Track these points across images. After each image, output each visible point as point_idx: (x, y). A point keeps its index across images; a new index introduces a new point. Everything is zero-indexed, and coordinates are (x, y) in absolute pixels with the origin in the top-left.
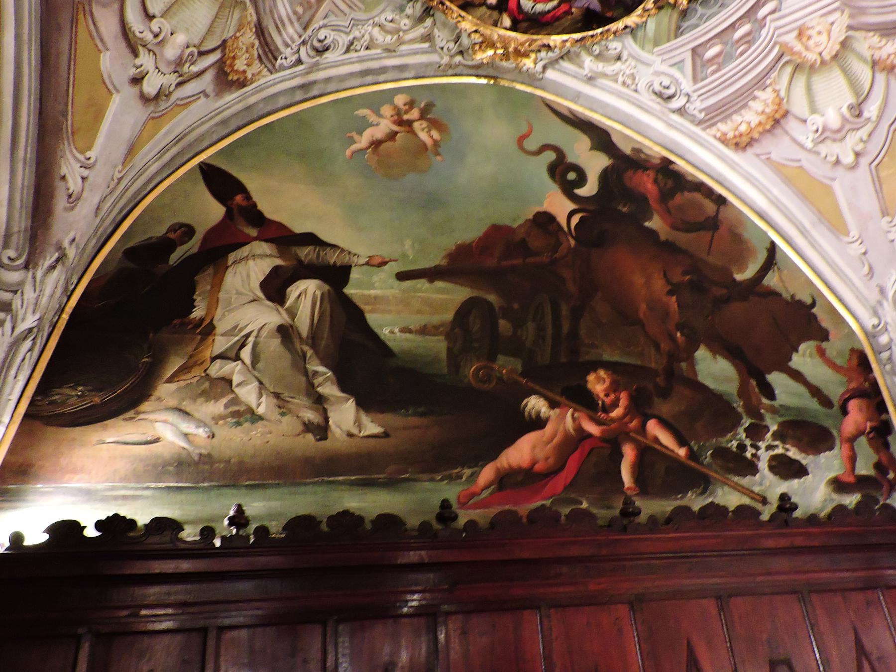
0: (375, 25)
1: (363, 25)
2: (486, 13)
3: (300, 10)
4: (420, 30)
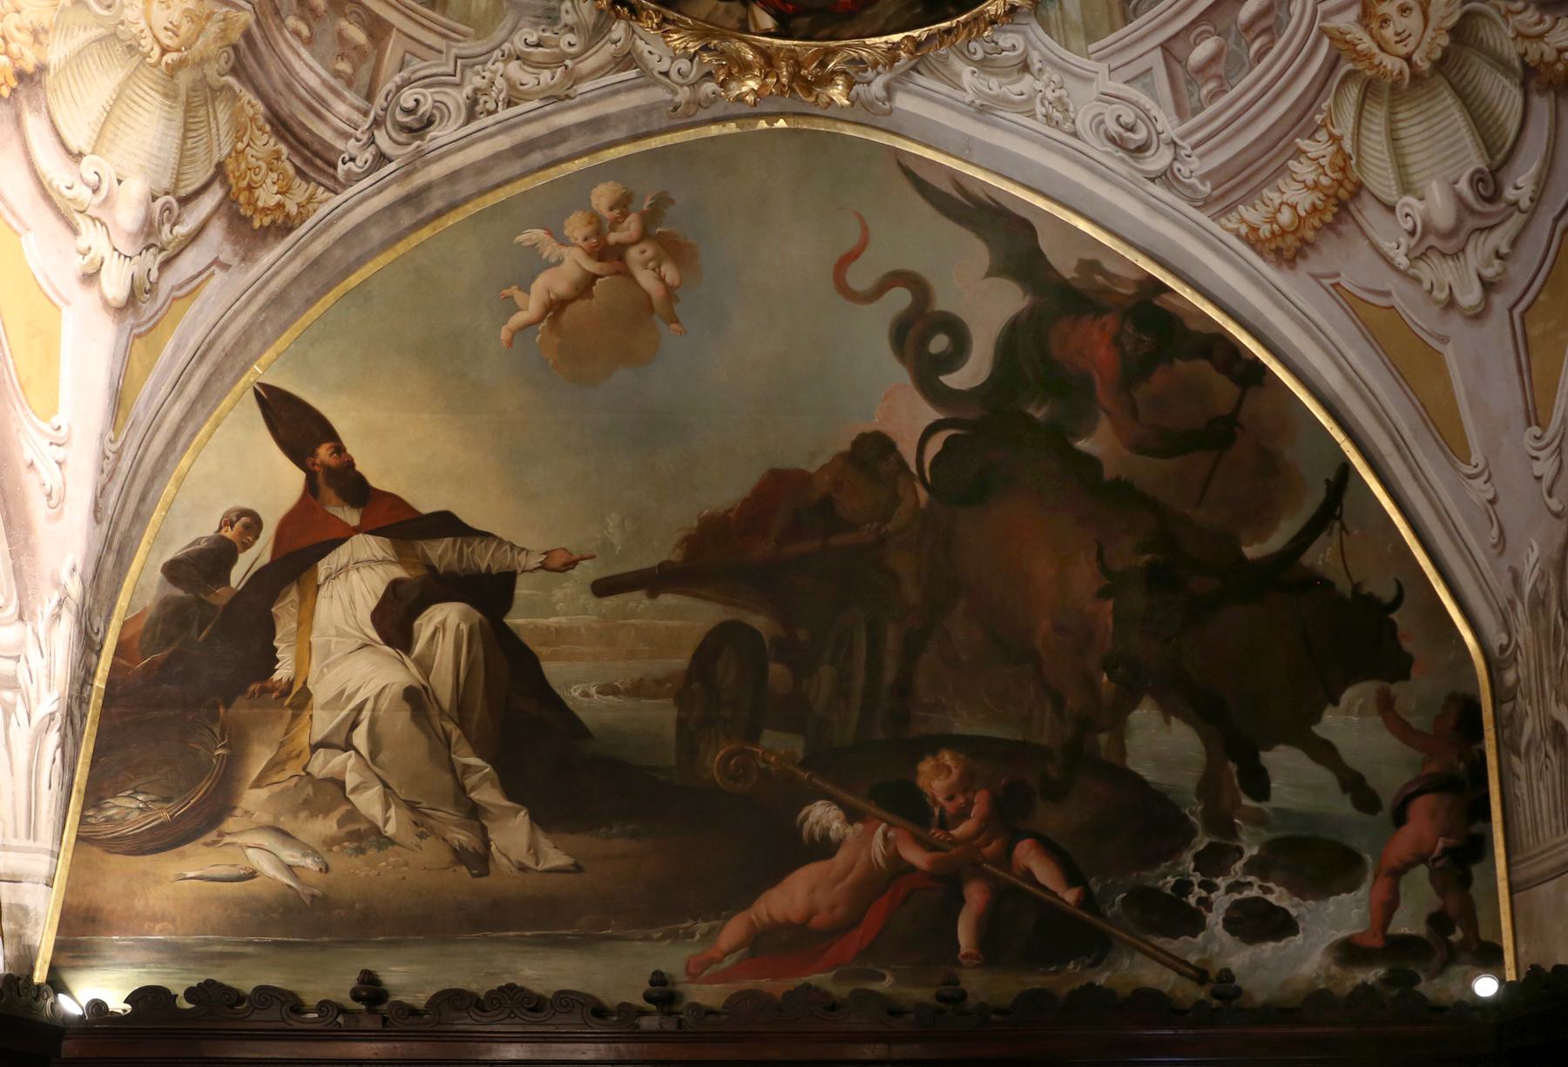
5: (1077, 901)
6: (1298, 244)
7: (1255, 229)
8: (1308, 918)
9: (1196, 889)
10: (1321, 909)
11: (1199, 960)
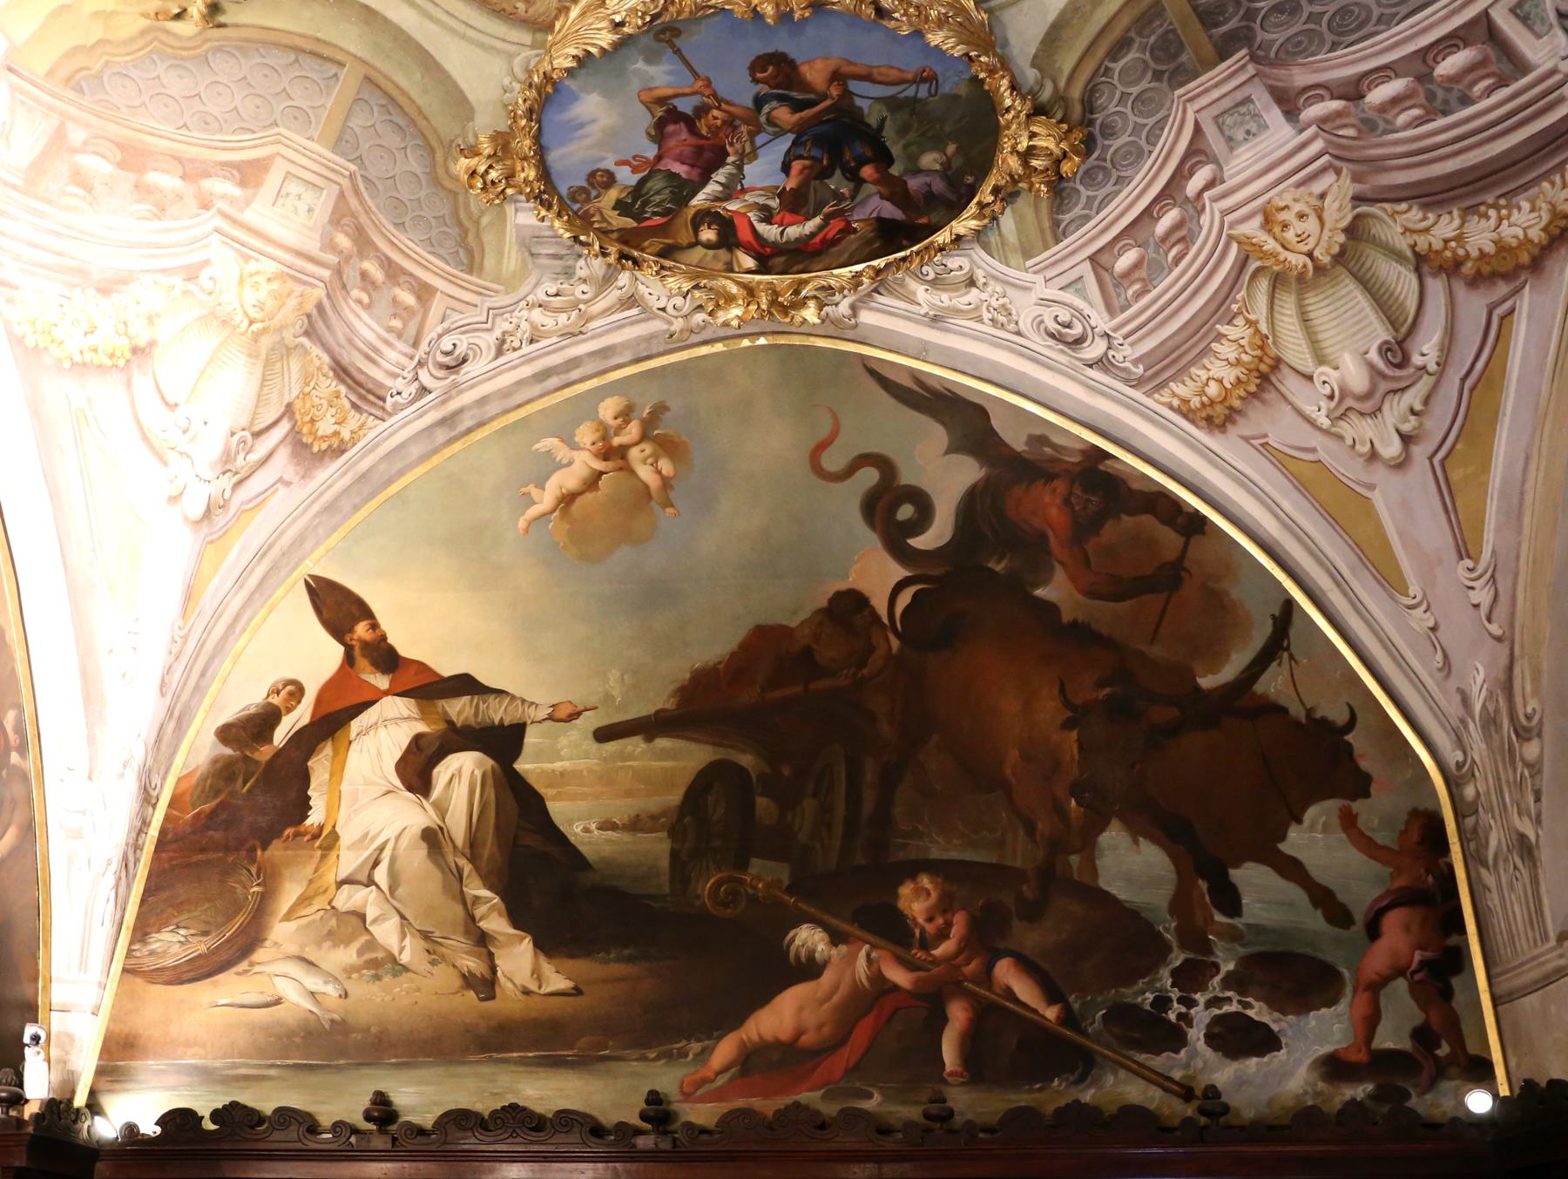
3: (397, 323)
4: (613, 296)
5: (1058, 1018)
6: (1227, 412)
7: (1186, 402)
8: (1290, 1033)
9: (1175, 1005)
10: (1302, 1024)
11: (1184, 1077)
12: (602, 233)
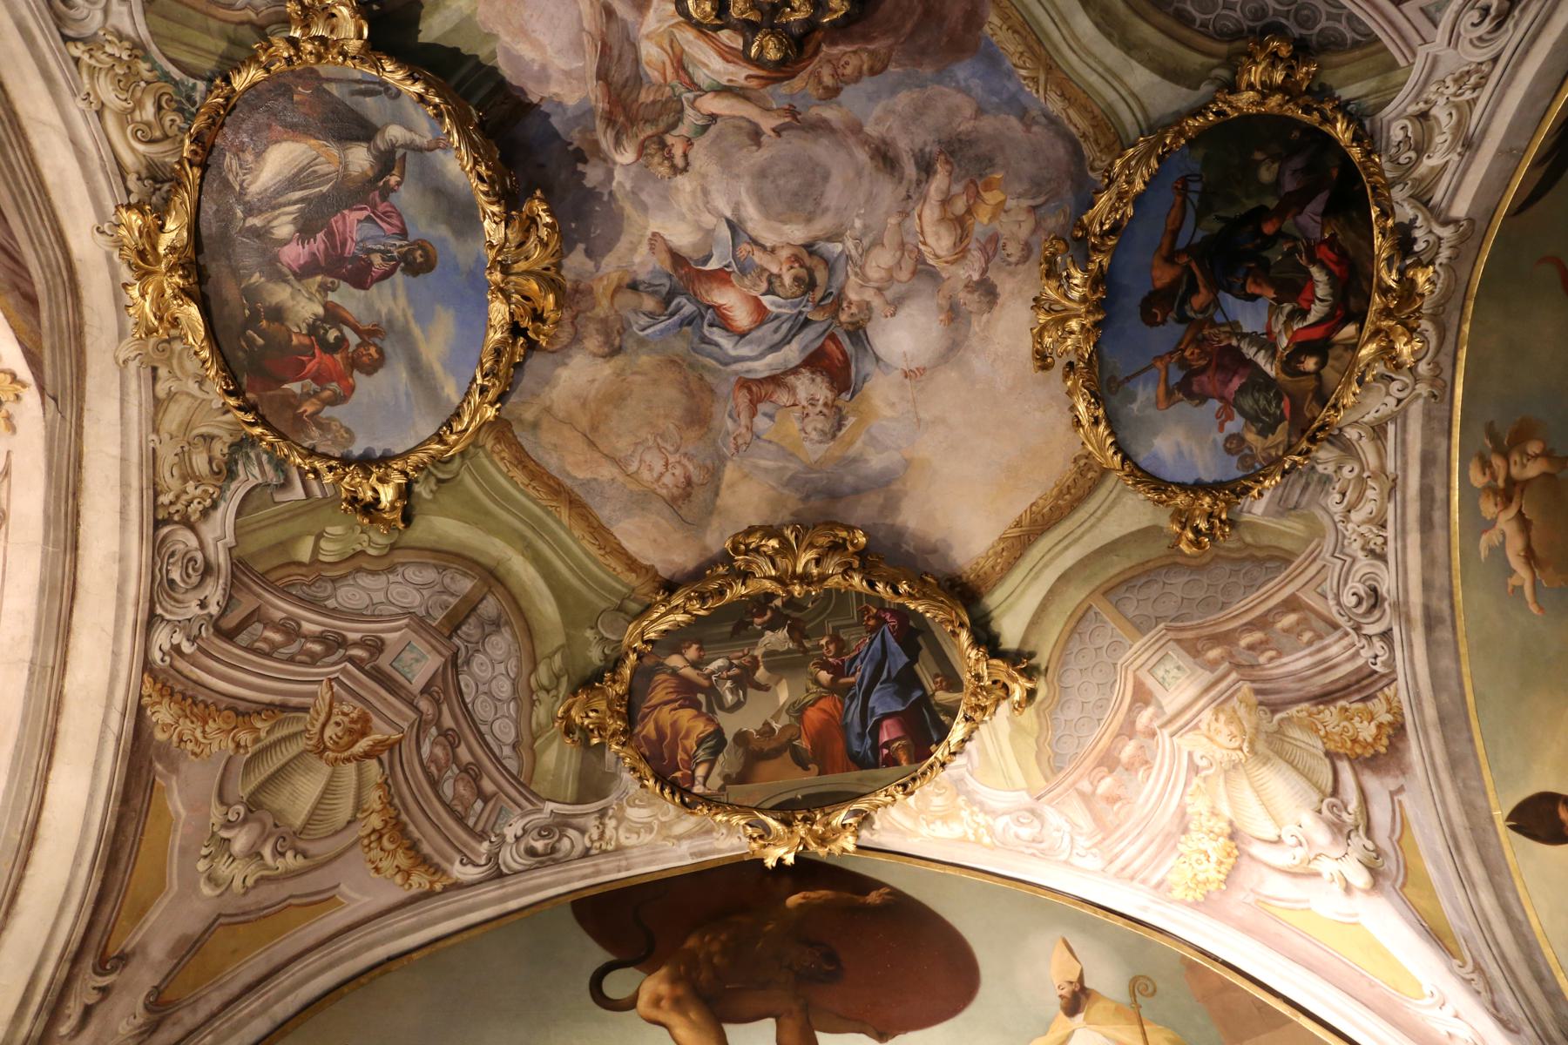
0: (1346, 518)
1: (1344, 537)
2: (1332, 367)
3: (1307, 636)
12: (1289, 449)
